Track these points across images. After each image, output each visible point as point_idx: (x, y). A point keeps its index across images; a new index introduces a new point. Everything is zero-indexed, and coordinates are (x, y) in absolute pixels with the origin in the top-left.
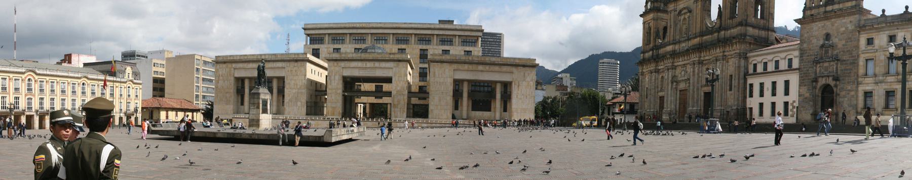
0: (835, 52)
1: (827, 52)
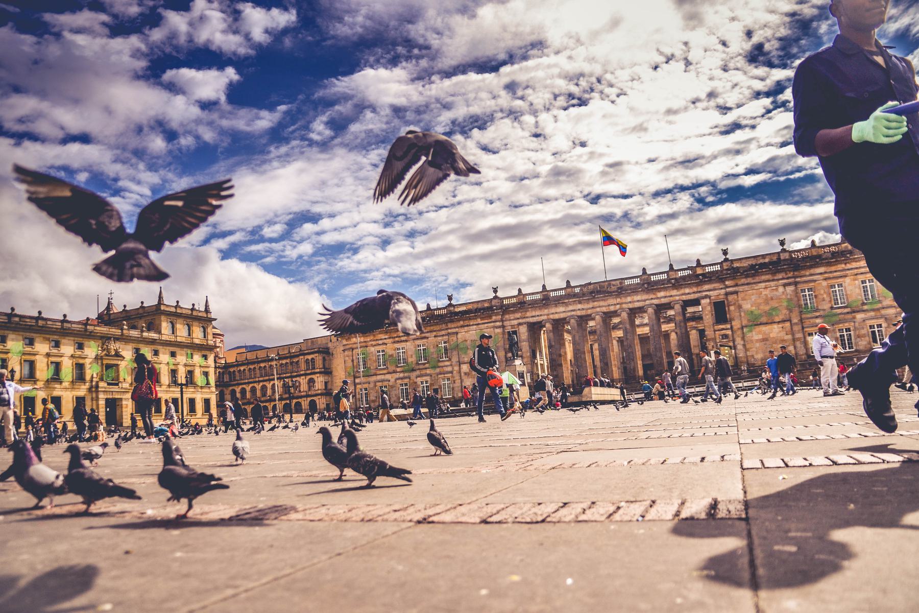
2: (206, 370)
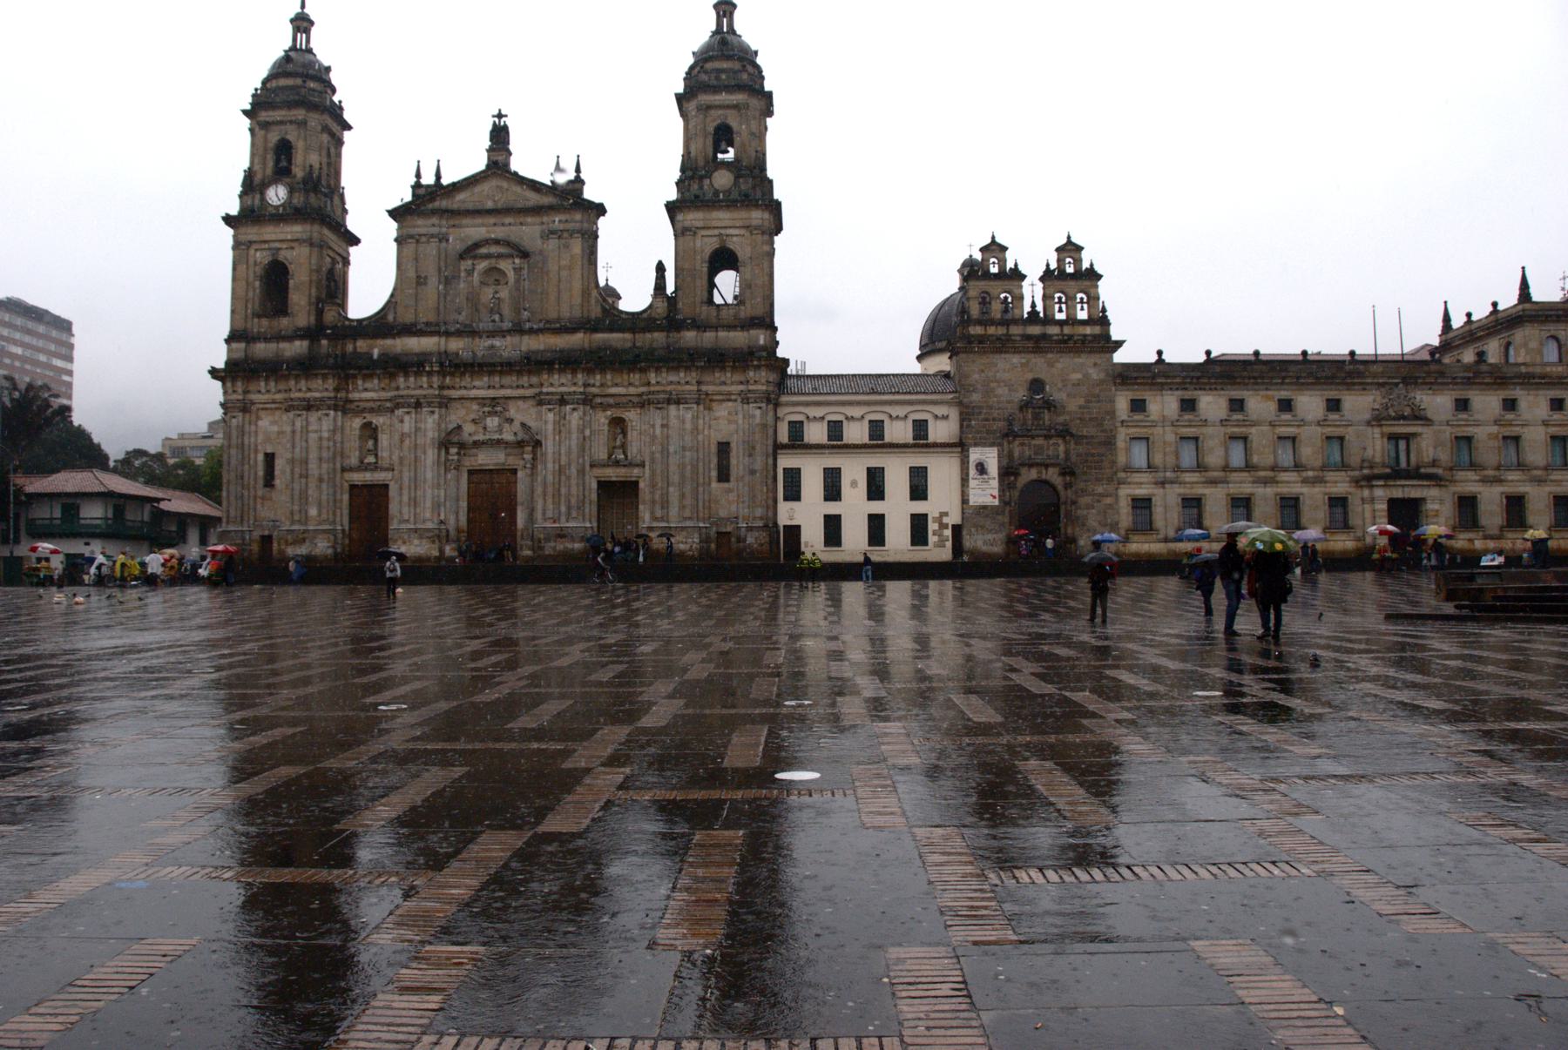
0: (1061, 419)
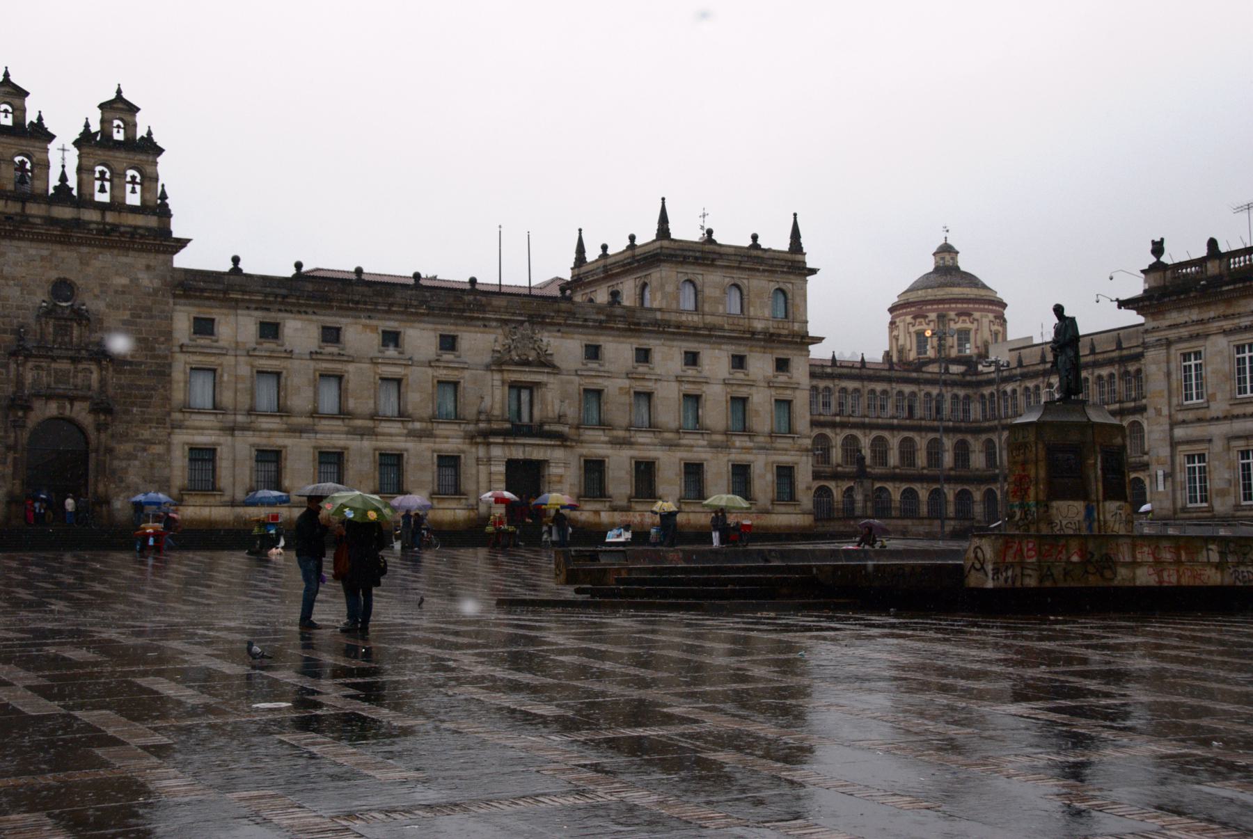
1: (62, 330)
2: (787, 395)
